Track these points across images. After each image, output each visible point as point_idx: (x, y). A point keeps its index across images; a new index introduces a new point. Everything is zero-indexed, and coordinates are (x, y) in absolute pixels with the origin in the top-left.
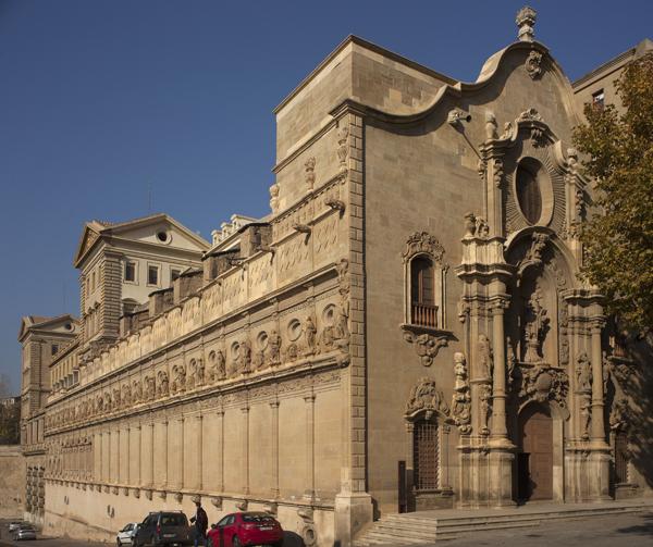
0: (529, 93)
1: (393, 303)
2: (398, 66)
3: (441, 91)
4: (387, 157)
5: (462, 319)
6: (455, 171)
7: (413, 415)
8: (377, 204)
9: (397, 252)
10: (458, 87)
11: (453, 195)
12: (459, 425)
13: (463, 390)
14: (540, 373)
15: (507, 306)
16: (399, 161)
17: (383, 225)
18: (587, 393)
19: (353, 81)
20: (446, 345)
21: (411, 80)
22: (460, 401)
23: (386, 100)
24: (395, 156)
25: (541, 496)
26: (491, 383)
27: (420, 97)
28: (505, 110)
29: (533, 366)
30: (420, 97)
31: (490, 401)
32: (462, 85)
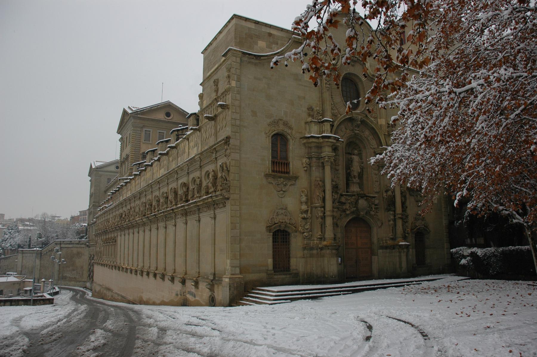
4: (255, 78)
5: (305, 169)
12: (304, 233)
13: (306, 212)
19: (235, 38)
26: (324, 207)
27: (277, 44)
30: (277, 44)
31: (324, 218)
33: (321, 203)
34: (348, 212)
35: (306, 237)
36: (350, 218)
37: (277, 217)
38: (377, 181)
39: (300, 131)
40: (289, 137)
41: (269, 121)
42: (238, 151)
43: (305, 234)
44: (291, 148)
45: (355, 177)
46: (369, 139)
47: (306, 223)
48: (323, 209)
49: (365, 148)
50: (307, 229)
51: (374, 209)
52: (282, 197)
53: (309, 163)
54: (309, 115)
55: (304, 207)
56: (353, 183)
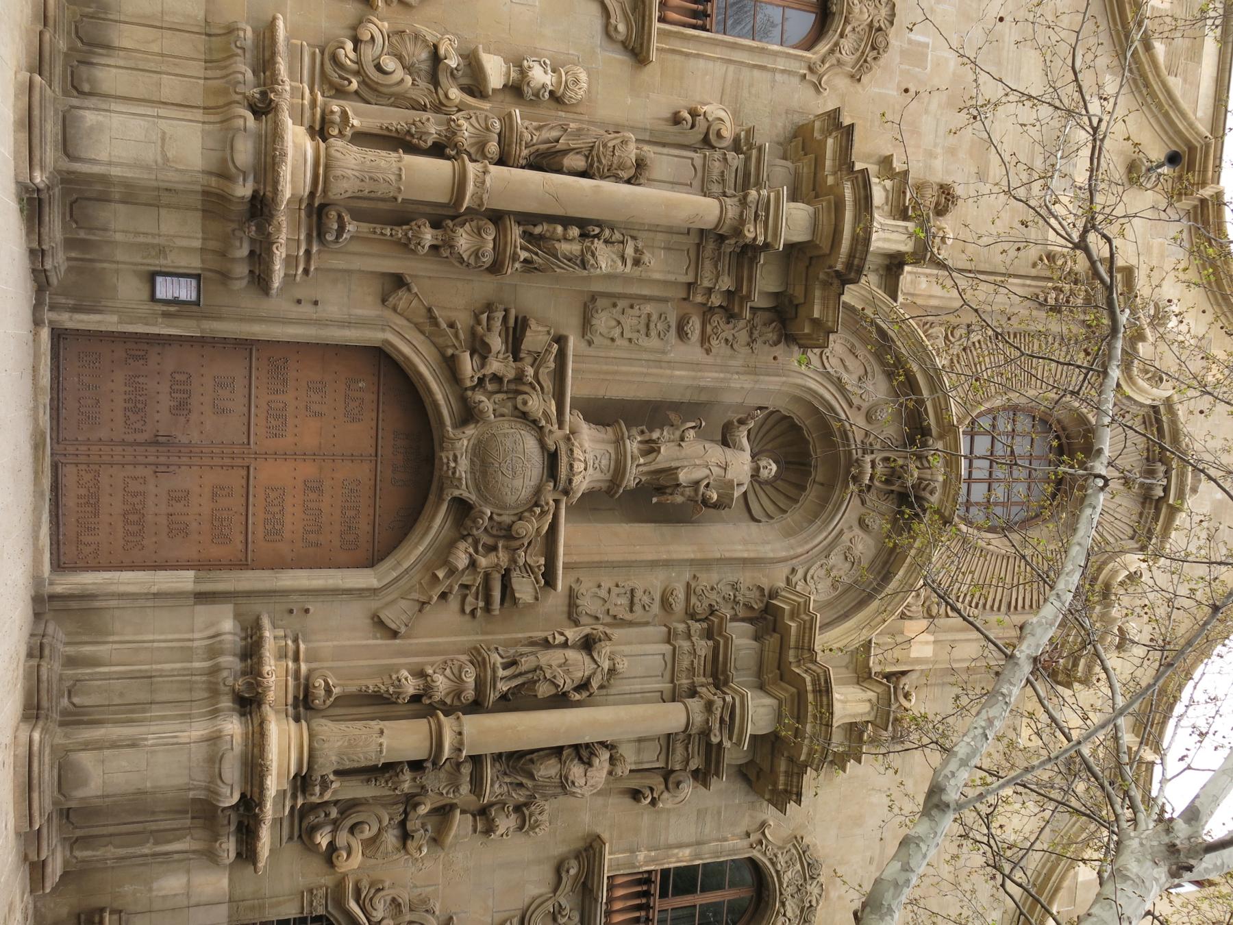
12: (357, 42)
13: (475, 86)
18: (480, 685)
22: (436, 58)
25: (70, 501)
34: (468, 365)
35: (335, 59)
36: (439, 391)
40: (823, 48)
43: (349, 45)
45: (651, 448)
47: (408, 68)
48: (493, 147)
49: (789, 533)
50: (379, 68)
53: (712, 137)
55: (496, 71)
56: (619, 442)
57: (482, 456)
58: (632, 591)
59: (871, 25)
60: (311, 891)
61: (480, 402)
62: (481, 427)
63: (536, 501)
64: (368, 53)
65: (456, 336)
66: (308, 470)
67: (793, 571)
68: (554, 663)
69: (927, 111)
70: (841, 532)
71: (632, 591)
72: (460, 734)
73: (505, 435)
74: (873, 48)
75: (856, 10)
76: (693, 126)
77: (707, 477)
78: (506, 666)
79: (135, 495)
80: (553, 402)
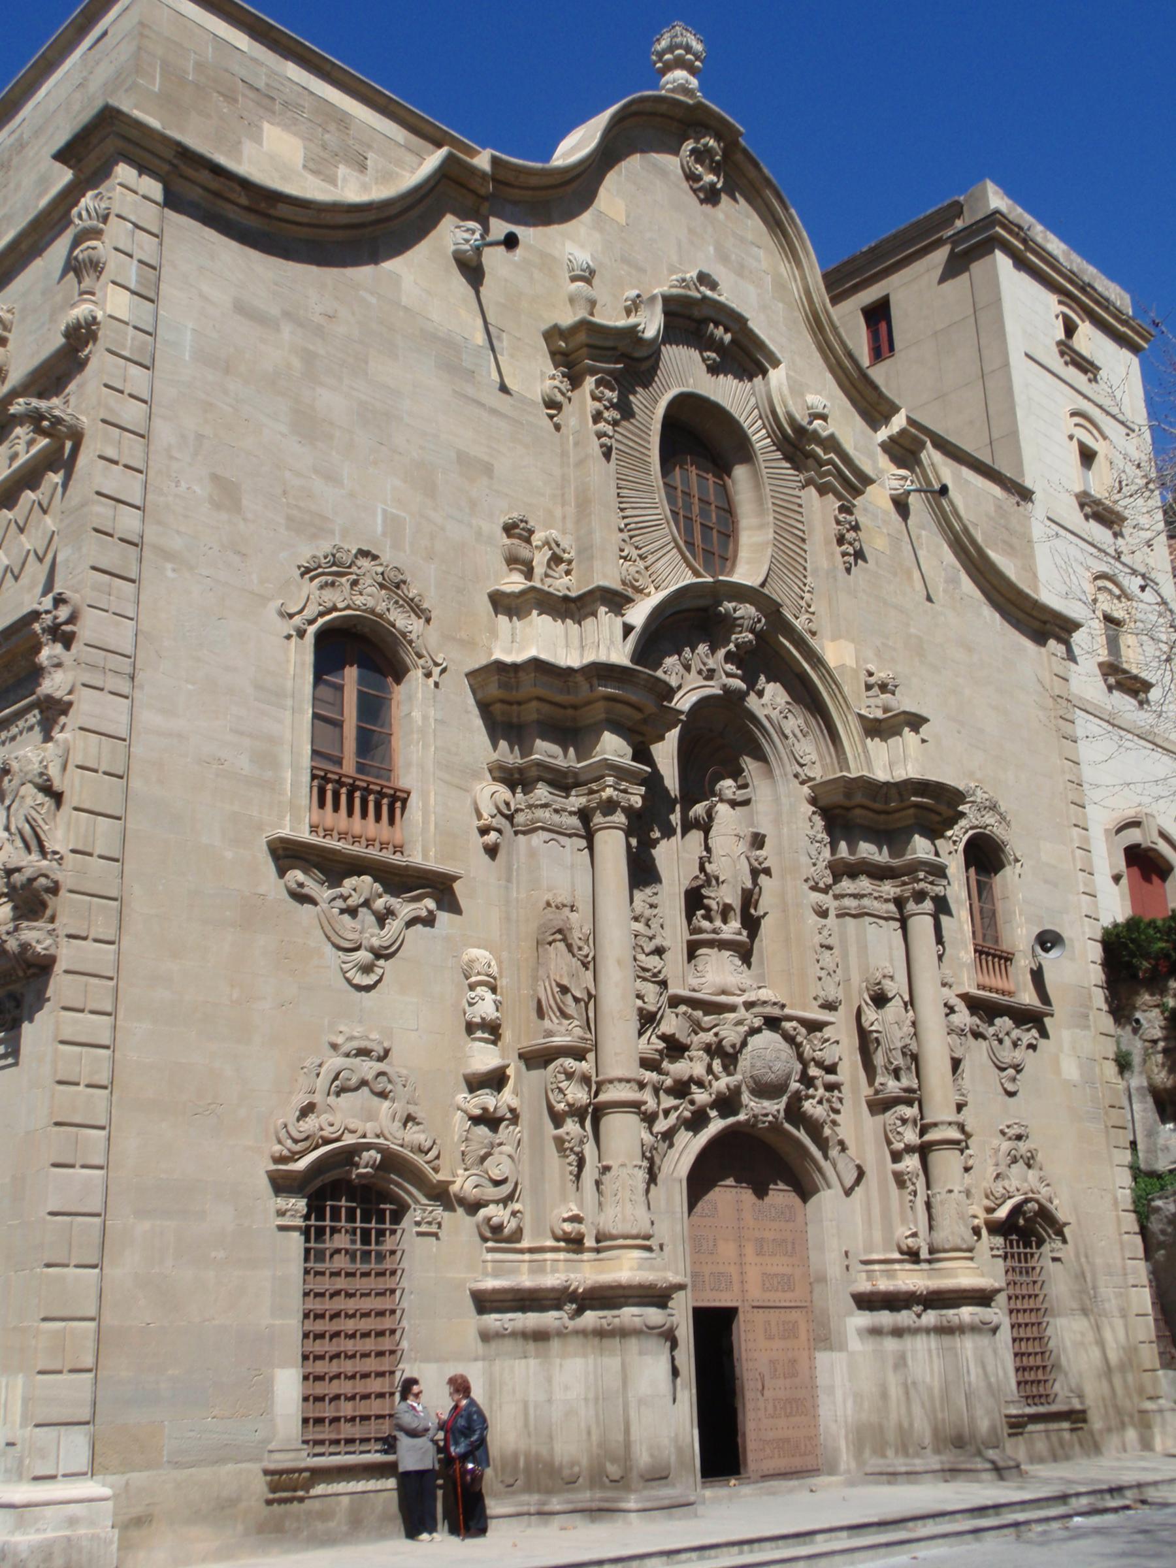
0: (691, 231)
1: (244, 764)
2: (293, 71)
3: (434, 159)
4: (241, 308)
6: (470, 391)
7: (302, 1164)
8: (200, 437)
9: (264, 599)
10: (482, 161)
11: (464, 460)
14: (754, 1031)
15: (637, 802)
16: (287, 329)
17: (218, 506)
20: (429, 921)
21: (343, 120)
23: (248, 147)
24: (275, 311)
27: (362, 167)
28: (625, 260)
29: (732, 1008)
30: (362, 167)
32: (495, 161)
33: (578, 1032)
37: (332, 1099)
38: (829, 948)
39: (463, 635)
41: (306, 553)
42: (124, 687)
44: (416, 715)
46: (787, 732)
50: (497, 1183)
51: (821, 1091)
52: (359, 988)
54: (512, 561)
57: (765, 1090)
58: (822, 946)
59: (382, 586)
60: (992, 1249)
61: (728, 1086)
62: (744, 1088)
63: (790, 1039)
64: (492, 1192)
65: (676, 1108)
66: (749, 1250)
67: (796, 776)
68: (899, 1034)
69: (443, 529)
70: (767, 717)
71: (822, 946)
72: (950, 1124)
73: (753, 1066)
74: (398, 587)
75: (371, 603)
76: (499, 831)
77: (748, 858)
78: (898, 1078)
79: (775, 1407)
80: (726, 1015)
